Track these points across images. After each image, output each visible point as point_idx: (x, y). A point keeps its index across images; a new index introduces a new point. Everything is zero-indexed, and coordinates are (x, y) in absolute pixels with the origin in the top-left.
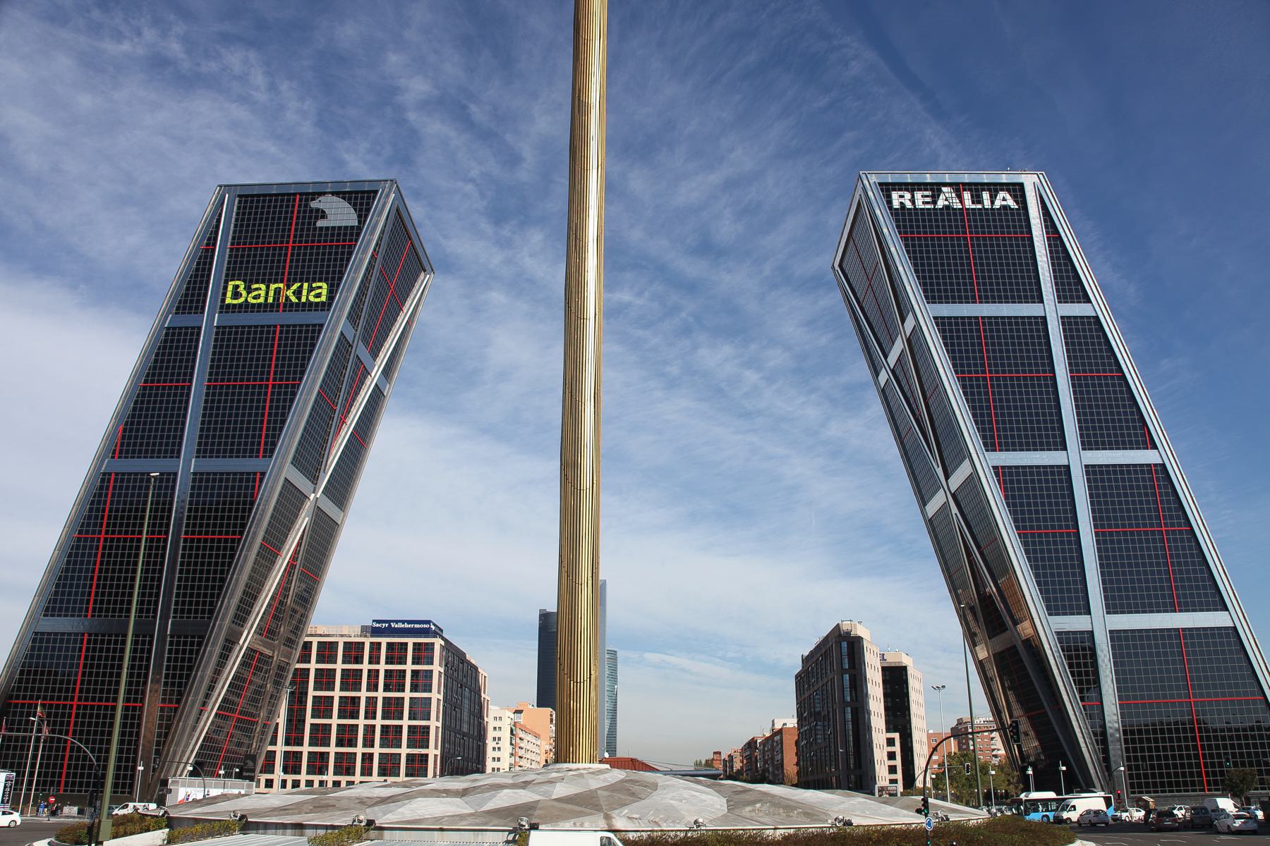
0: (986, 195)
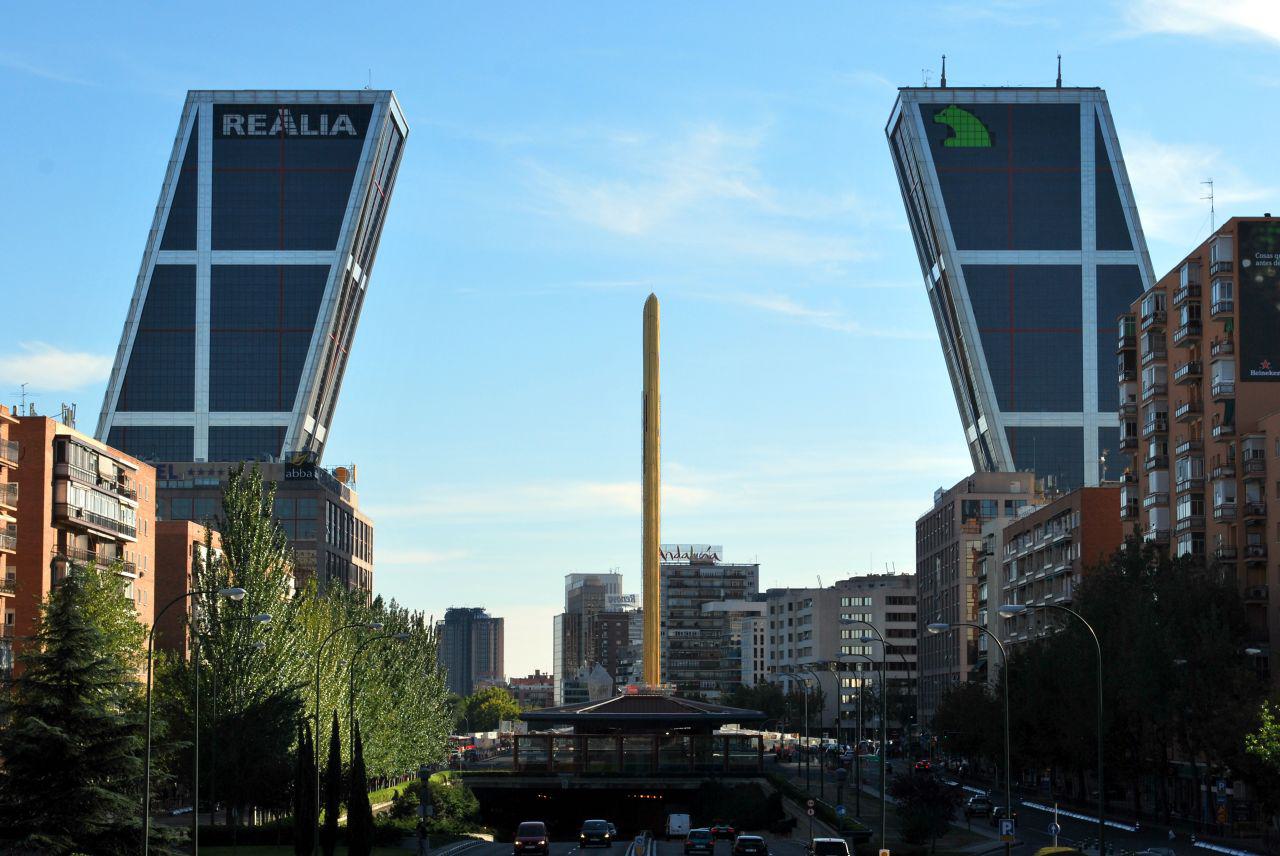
0: (324, 119)
